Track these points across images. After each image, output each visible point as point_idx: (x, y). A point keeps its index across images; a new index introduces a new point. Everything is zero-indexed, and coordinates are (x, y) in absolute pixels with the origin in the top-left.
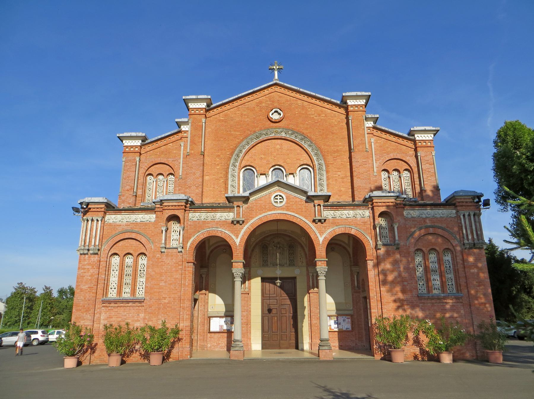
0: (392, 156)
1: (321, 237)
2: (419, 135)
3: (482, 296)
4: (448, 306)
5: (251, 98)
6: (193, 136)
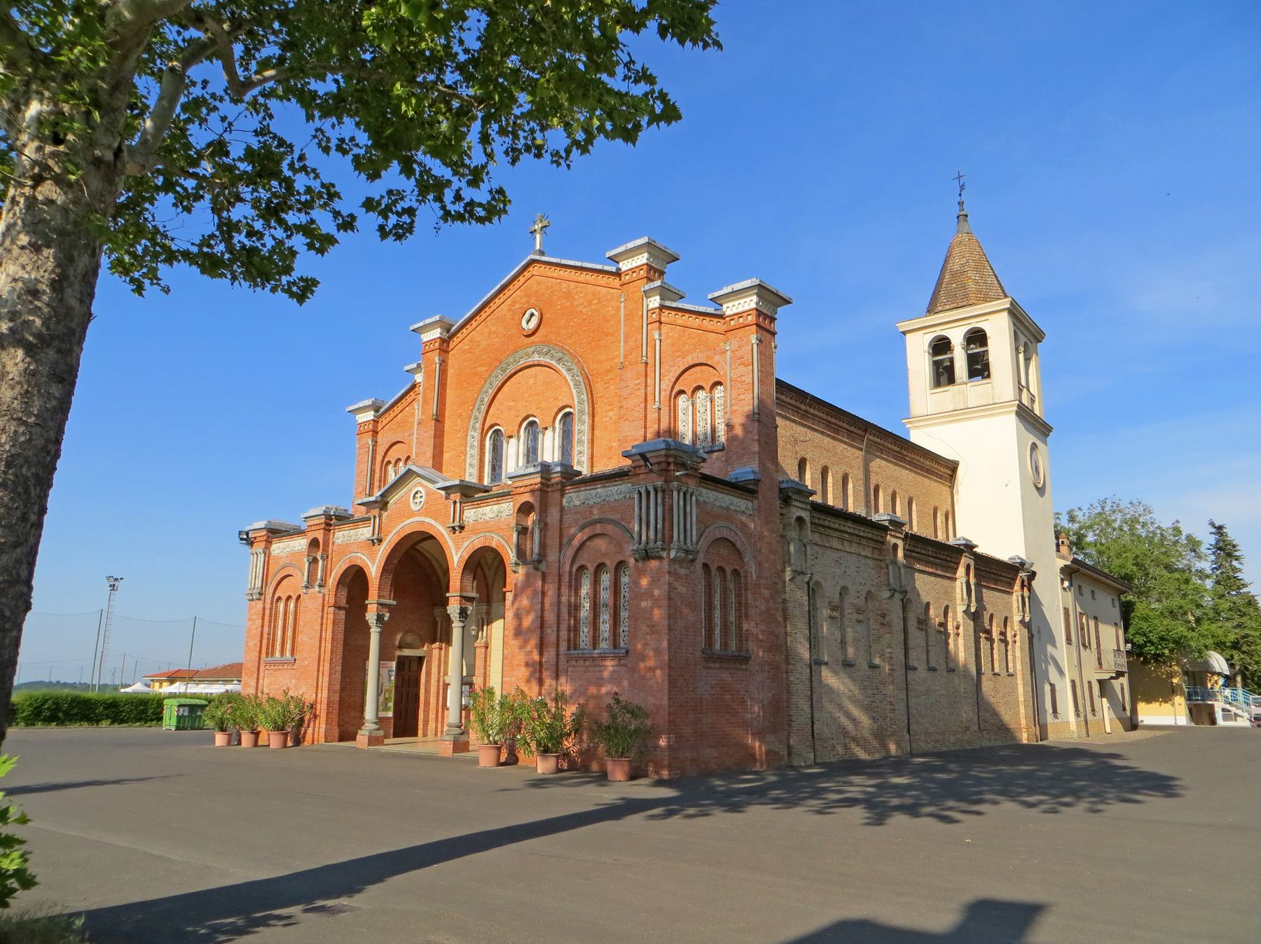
0: (690, 360)
1: (457, 554)
2: (730, 305)
3: (651, 654)
4: (606, 674)
5: (502, 297)
6: (425, 389)
